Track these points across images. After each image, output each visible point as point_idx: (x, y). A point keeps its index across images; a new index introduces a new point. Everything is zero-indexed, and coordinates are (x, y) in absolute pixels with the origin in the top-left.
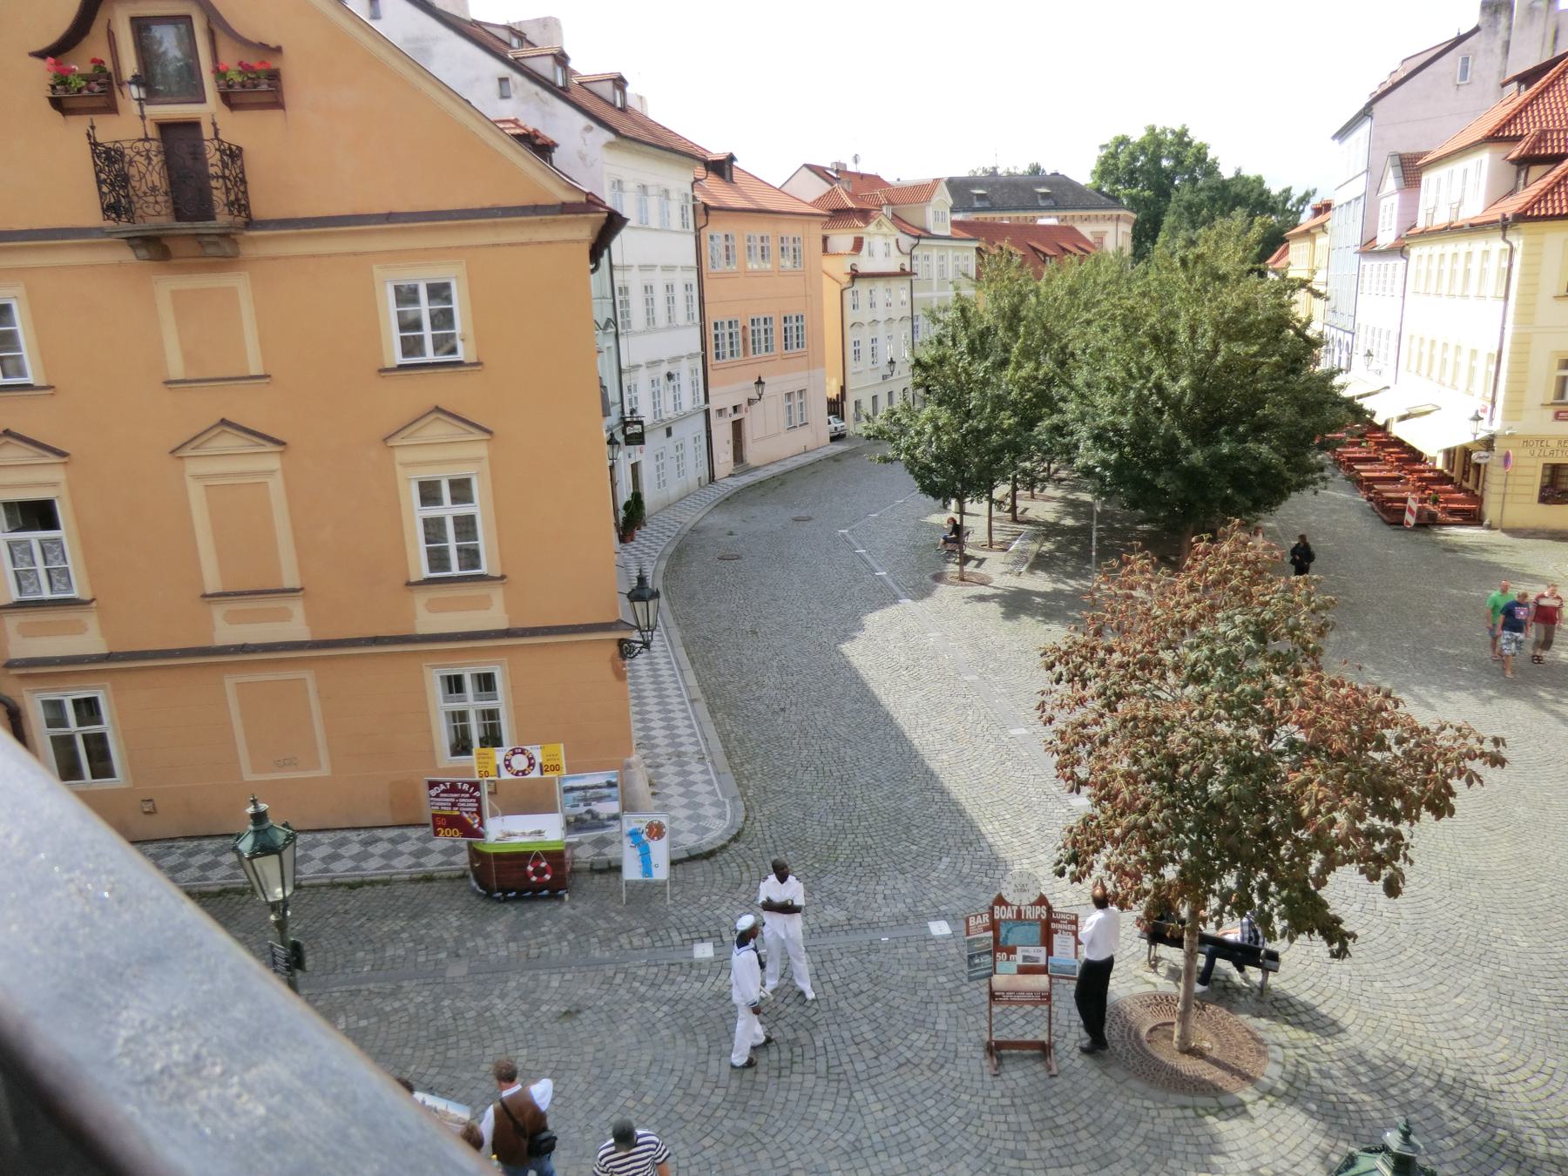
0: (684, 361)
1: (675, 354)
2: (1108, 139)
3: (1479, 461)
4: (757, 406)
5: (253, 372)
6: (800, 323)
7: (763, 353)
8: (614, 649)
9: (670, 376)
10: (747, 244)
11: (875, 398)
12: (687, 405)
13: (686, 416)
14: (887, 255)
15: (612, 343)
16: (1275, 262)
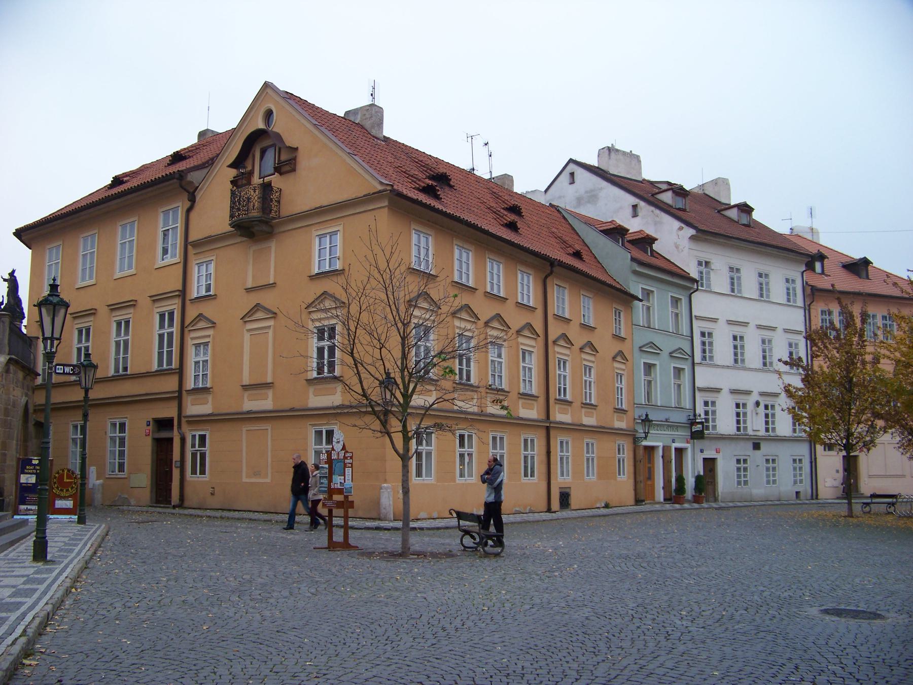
5: (271, 283)
9: (758, 404)
15: (686, 367)
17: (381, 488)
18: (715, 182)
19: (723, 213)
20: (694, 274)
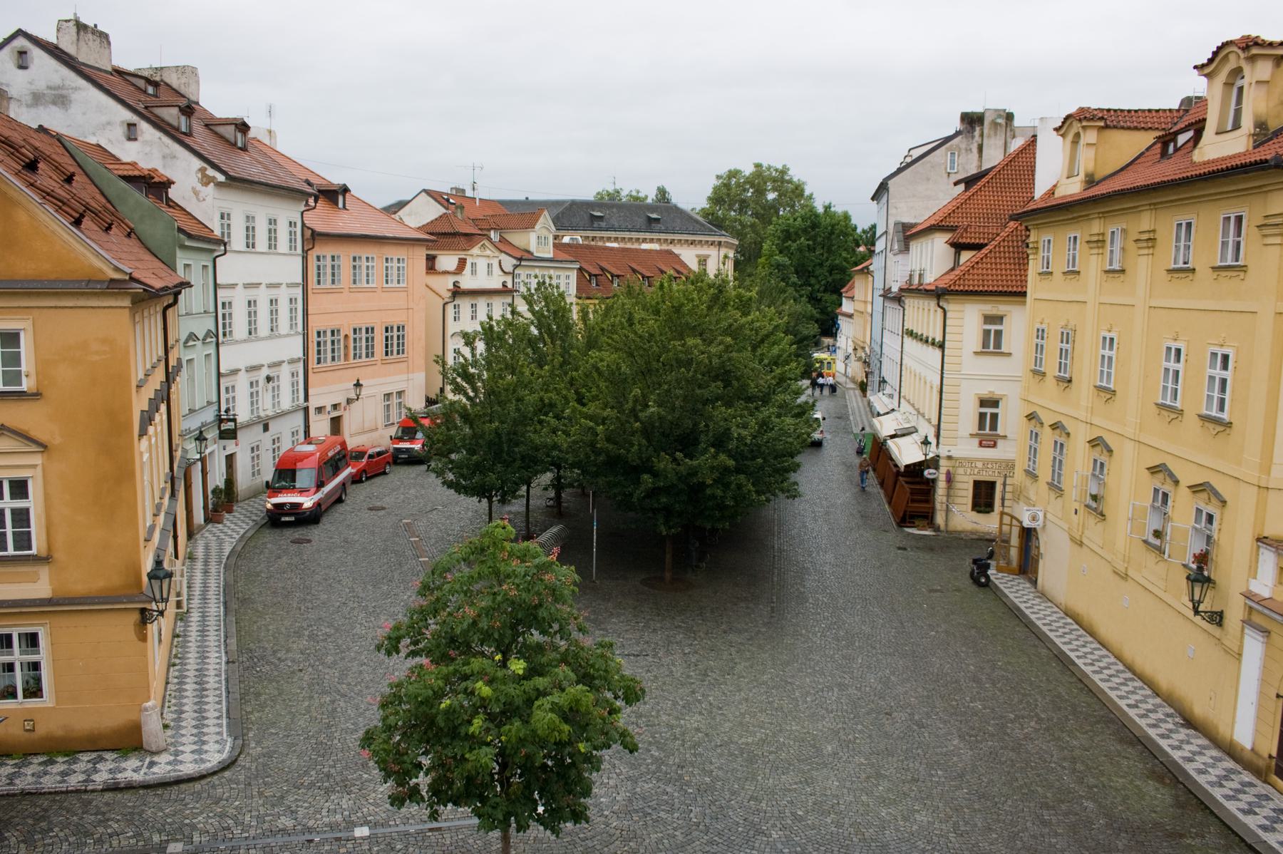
0: (285, 365)
1: (276, 360)
2: (723, 171)
3: (929, 477)
4: (355, 405)
6: (401, 333)
7: (364, 359)
8: (136, 617)
9: (269, 379)
10: (352, 263)
12: (286, 403)
13: (283, 414)
14: (490, 272)
15: (212, 350)
18: (182, 70)
19: (212, 127)
20: (217, 232)
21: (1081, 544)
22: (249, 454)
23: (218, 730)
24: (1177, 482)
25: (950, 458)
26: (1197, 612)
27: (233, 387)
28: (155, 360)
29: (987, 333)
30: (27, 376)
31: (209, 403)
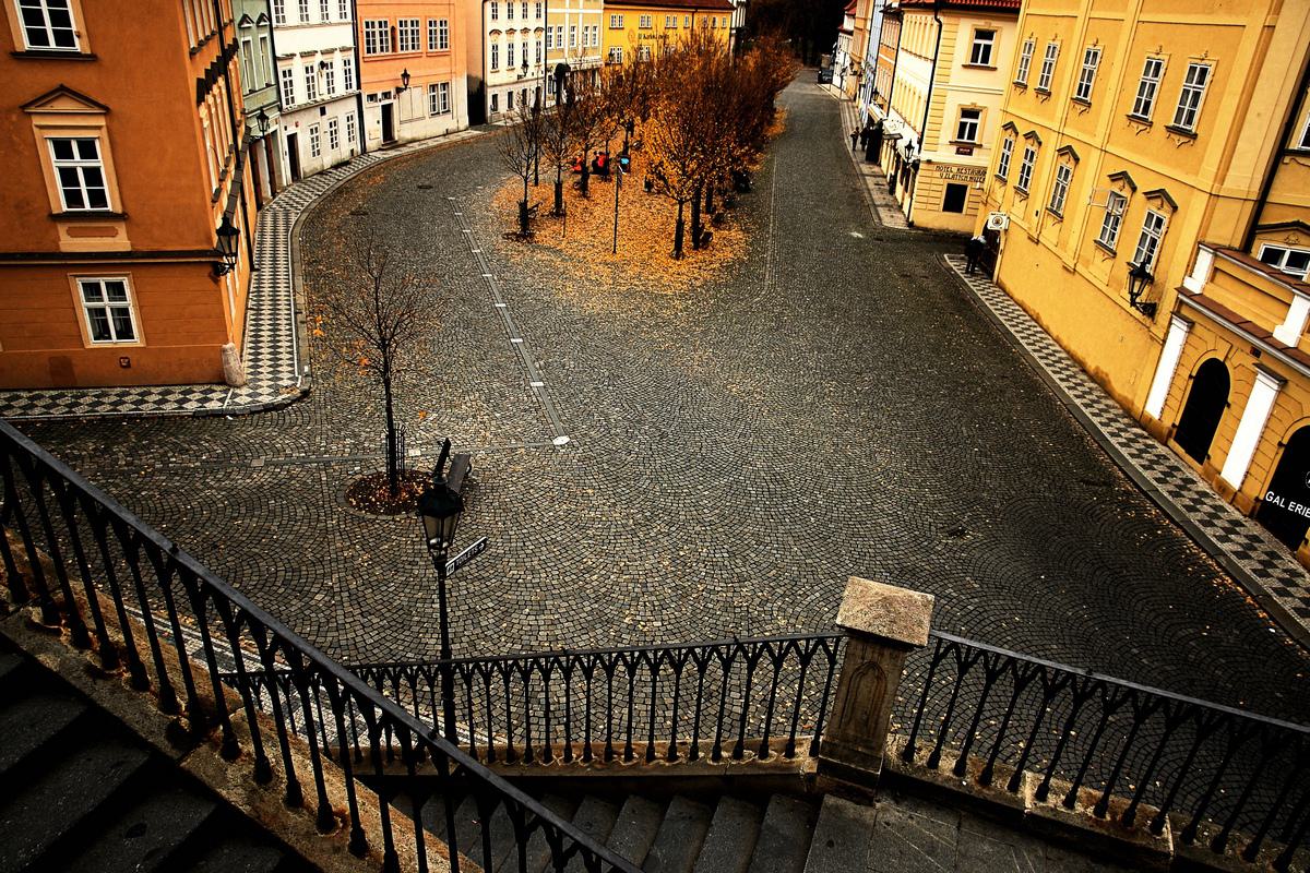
0: (337, 53)
6: (444, 28)
8: (209, 269)
9: (323, 65)
11: (510, 94)
12: (340, 90)
15: (266, 34)
16: (848, 10)
17: (224, 351)
21: (1038, 242)
22: (308, 136)
23: (290, 369)
24: (1134, 189)
25: (929, 162)
26: (1133, 303)
27: (290, 71)
28: (208, 33)
29: (977, 47)
30: (79, 36)
31: (268, 85)
